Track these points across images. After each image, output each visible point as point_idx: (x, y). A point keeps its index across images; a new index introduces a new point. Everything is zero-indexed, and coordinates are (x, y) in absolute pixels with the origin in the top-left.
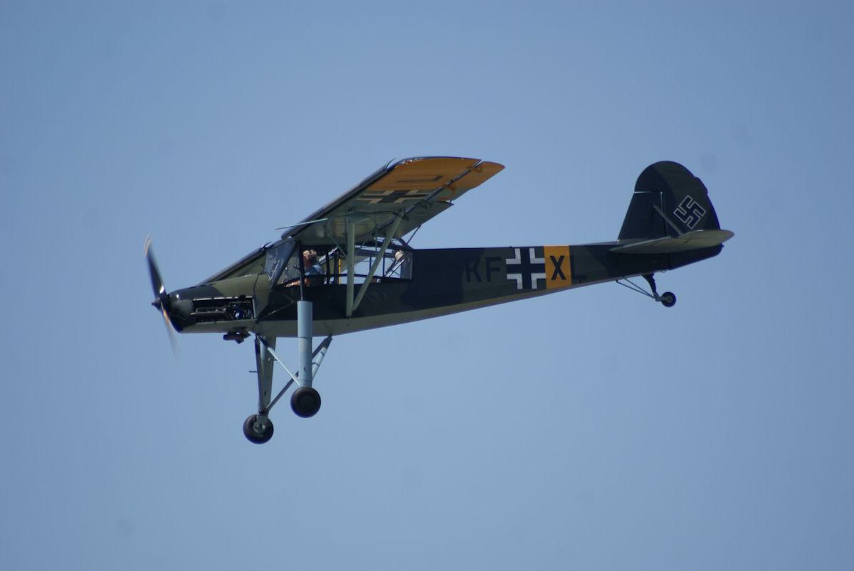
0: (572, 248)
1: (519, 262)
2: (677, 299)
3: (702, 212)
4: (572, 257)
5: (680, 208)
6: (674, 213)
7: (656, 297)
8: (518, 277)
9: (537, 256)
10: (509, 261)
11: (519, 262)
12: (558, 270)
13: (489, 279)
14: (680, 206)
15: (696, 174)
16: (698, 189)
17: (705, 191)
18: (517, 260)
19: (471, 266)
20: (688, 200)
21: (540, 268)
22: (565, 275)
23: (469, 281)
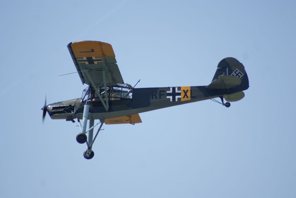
0: (191, 87)
1: (172, 92)
3: (242, 74)
4: (191, 90)
8: (171, 97)
10: (168, 92)
11: (172, 92)
12: (186, 95)
13: (160, 98)
14: (234, 73)
15: (240, 62)
16: (241, 67)
17: (243, 67)
18: (171, 91)
19: (154, 94)
20: (237, 70)
21: (179, 94)
22: (188, 96)
23: (153, 98)
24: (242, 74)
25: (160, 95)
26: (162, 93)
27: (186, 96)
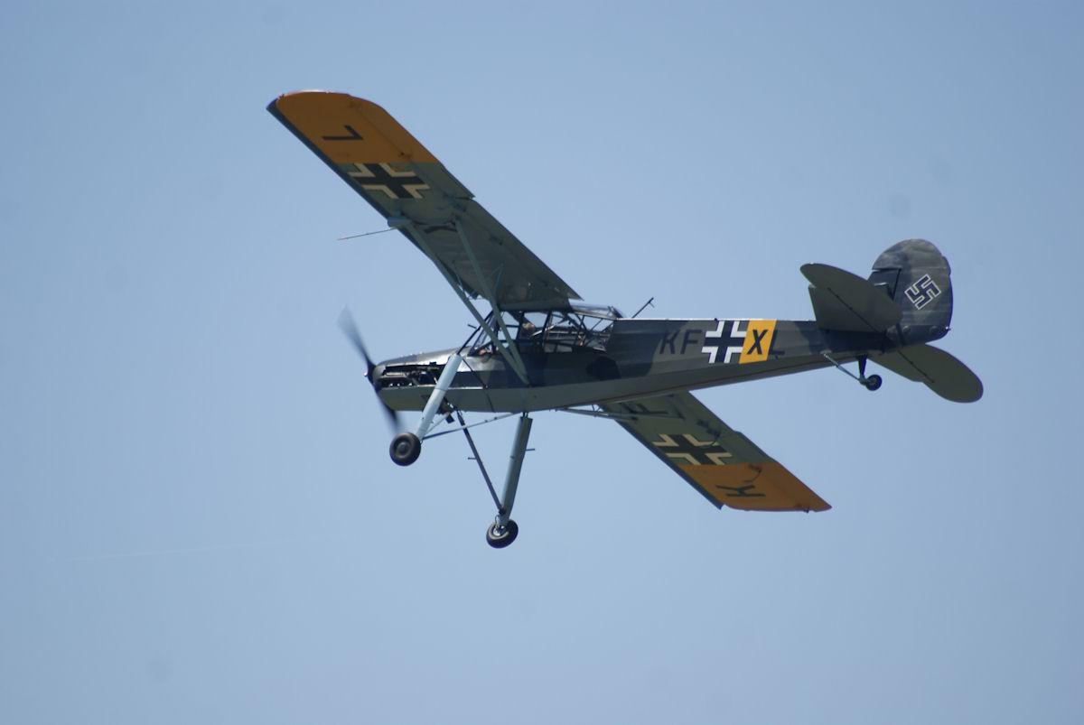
1: (720, 335)
2: (883, 382)
3: (936, 292)
4: (775, 332)
5: (914, 288)
6: (906, 292)
7: (863, 381)
8: (713, 351)
9: (739, 330)
10: (710, 334)
12: (757, 345)
13: (683, 352)
16: (938, 265)
18: (718, 333)
19: (669, 338)
20: (926, 278)
21: (740, 342)
23: (662, 351)
24: (936, 292)
25: (686, 341)
26: (691, 337)
27: (756, 350)
